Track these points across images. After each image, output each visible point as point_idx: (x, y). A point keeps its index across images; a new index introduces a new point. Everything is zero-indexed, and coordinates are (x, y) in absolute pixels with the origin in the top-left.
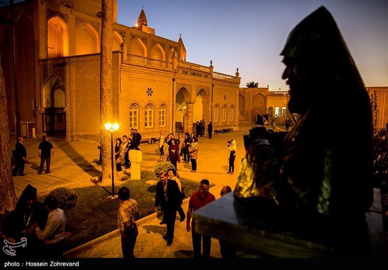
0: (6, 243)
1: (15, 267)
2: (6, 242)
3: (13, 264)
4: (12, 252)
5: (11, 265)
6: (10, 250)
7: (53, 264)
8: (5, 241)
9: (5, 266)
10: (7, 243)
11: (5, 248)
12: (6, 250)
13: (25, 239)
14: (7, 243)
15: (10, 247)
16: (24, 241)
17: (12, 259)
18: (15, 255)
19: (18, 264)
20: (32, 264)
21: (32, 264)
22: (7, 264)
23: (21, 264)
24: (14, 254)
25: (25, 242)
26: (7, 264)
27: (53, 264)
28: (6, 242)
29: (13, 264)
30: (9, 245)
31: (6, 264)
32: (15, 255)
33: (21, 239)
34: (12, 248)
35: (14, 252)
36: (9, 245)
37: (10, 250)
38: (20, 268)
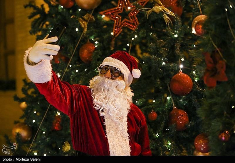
0: (4, 147)
1: (9, 161)
2: (4, 146)
3: (8, 160)
4: (7, 152)
5: (7, 160)
6: (6, 151)
7: (32, 159)
8: (4, 146)
9: (3, 160)
10: (5, 147)
11: (4, 150)
12: (4, 151)
13: (15, 144)
14: (5, 147)
15: (6, 149)
16: (15, 145)
17: (7, 157)
18: (10, 154)
19: (11, 160)
20: (20, 160)
21: (20, 160)
22: (4, 160)
23: (13, 160)
24: (9, 154)
25: (15, 146)
26: (4, 160)
27: (32, 159)
28: (4, 146)
29: (8, 160)
30: (6, 148)
31: (4, 160)
32: (10, 154)
33: (13, 145)
34: (8, 150)
35: (9, 152)
36: (6, 148)
37: (6, 151)
38: (12, 161)
